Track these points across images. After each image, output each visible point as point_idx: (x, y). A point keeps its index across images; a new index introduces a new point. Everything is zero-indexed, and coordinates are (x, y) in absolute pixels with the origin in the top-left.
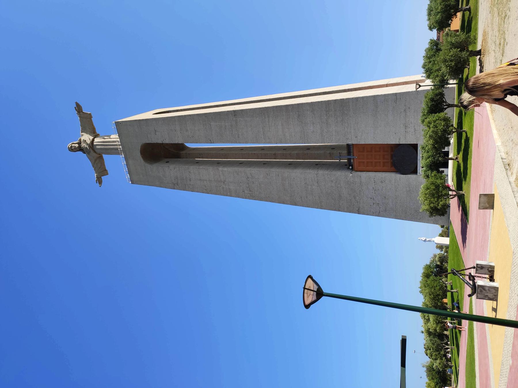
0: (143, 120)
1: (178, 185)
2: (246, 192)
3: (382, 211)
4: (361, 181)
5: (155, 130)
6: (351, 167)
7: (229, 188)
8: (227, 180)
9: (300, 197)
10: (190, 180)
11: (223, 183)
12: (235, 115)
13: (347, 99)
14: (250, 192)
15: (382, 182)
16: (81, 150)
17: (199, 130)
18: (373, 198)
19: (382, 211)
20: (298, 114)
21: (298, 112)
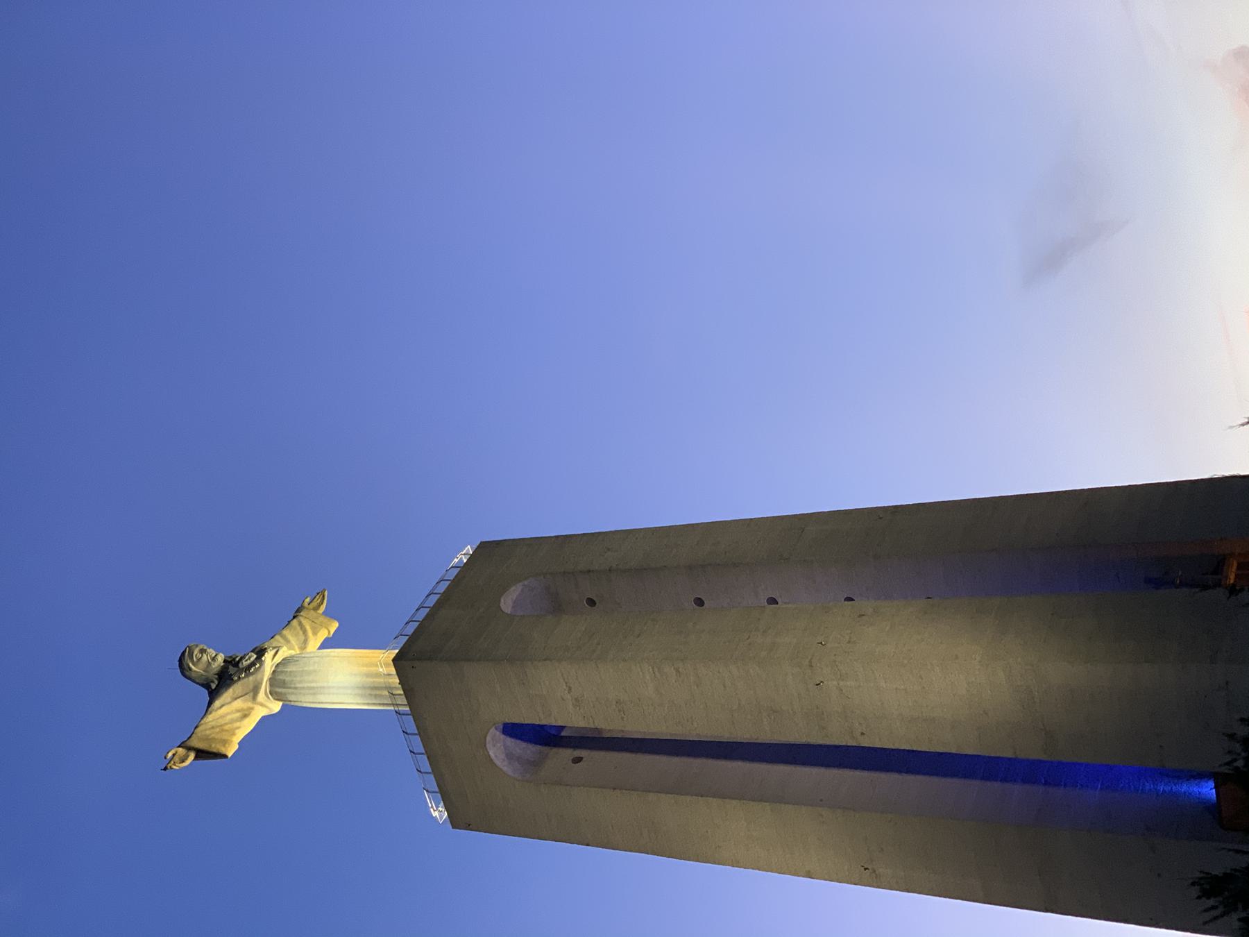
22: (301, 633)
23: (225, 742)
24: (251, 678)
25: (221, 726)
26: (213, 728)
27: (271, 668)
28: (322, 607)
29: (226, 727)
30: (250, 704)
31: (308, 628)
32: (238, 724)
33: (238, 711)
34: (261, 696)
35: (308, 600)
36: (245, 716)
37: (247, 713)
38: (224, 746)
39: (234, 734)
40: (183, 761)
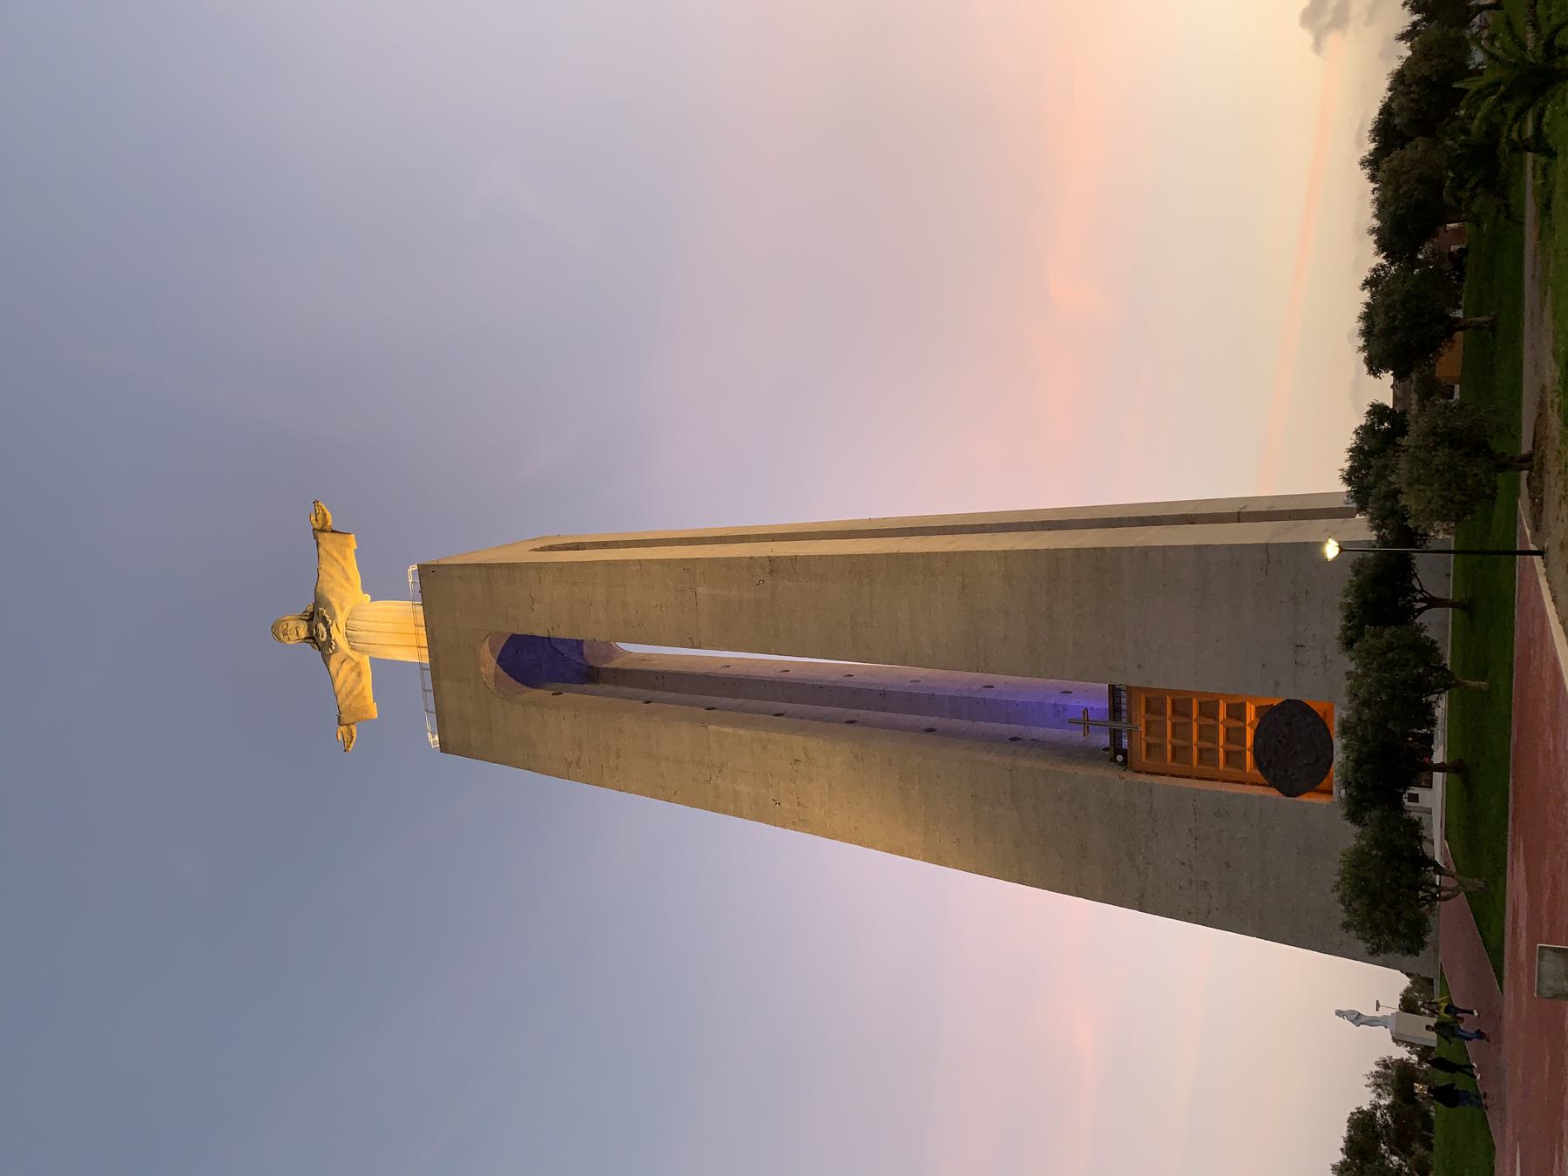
0: (500, 565)
1: (580, 768)
3: (1217, 909)
4: (1152, 805)
5: (531, 596)
6: (1120, 758)
7: (734, 790)
10: (618, 756)
12: (771, 571)
13: (1113, 549)
14: (797, 808)
15: (1217, 814)
16: (308, 640)
18: (1190, 865)
19: (1217, 909)
21: (963, 575)
22: (334, 562)
23: (365, 710)
24: (339, 654)
25: (351, 691)
26: (347, 696)
29: (356, 692)
31: (335, 553)
32: (360, 687)
33: (352, 670)
35: (313, 518)
36: (359, 674)
38: (366, 712)
39: (365, 697)
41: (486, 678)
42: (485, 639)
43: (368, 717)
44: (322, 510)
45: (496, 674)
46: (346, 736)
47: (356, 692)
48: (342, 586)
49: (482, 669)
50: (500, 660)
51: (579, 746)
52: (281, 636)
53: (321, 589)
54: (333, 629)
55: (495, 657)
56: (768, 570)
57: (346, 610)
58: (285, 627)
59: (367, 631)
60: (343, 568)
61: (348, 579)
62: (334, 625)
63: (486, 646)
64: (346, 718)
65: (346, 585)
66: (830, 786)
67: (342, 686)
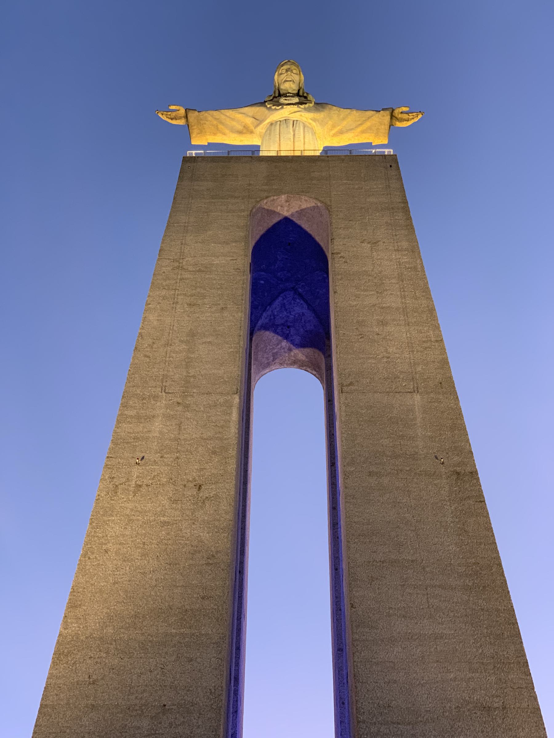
1: (173, 269)
2: (136, 471)
7: (154, 417)
8: (189, 415)
9: (95, 677)
11: (179, 400)
12: (458, 474)
17: (388, 358)
20: (496, 705)
21: (504, 708)
22: (359, 123)
23: (202, 132)
25: (221, 123)
27: (282, 118)
28: (405, 122)
29: (220, 126)
30: (253, 128)
31: (368, 124)
32: (227, 131)
34: (262, 128)
36: (240, 132)
37: (244, 131)
39: (215, 134)
40: (172, 119)
41: (274, 199)
42: (320, 201)
43: (193, 135)
44: (413, 119)
45: (274, 212)
46: (174, 114)
47: (220, 126)
48: (334, 126)
49: (283, 197)
50: (287, 221)
51: (200, 271)
52: (285, 67)
53: (331, 109)
54: (295, 108)
55: (292, 215)
56: (458, 469)
57: (314, 124)
58: (294, 71)
59: (294, 135)
60: (352, 129)
61: (341, 132)
62: (300, 109)
63: (306, 203)
64: (193, 116)
65: (333, 132)
66: (165, 523)
67: (226, 116)
